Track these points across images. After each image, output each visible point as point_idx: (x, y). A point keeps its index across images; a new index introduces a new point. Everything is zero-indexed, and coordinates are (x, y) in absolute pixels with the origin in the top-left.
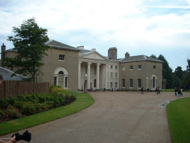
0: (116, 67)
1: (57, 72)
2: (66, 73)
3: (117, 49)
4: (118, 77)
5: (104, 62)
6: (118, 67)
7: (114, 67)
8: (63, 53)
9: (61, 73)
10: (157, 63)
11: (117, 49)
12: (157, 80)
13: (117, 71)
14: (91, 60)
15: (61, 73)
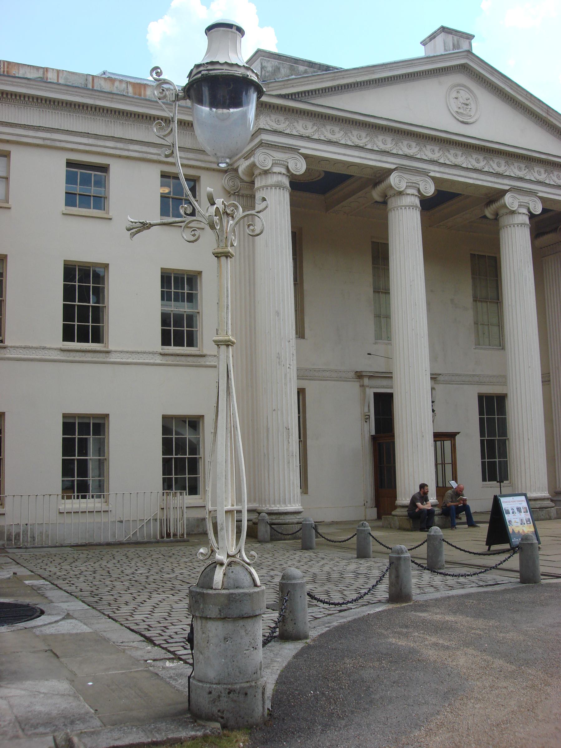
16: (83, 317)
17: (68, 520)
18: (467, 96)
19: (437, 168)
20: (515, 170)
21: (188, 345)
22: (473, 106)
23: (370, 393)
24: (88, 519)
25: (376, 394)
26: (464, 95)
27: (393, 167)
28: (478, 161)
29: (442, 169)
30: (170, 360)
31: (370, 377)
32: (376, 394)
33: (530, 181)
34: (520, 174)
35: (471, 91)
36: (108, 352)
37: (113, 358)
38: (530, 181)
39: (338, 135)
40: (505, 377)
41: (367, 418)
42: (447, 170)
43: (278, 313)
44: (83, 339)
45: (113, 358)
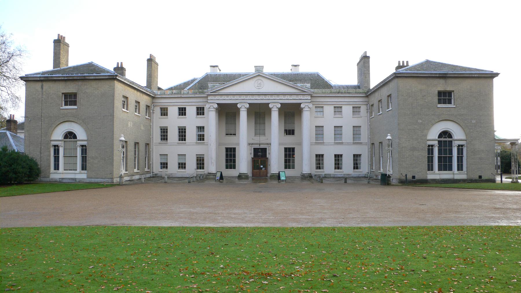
0: (356, 109)
1: (58, 134)
2: (81, 134)
3: (368, 57)
4: (365, 136)
5: (295, 97)
6: (363, 109)
7: (347, 110)
8: (70, 88)
9: (70, 135)
10: (450, 81)
11: (368, 57)
12: (461, 143)
13: (362, 120)
14: (249, 97)
15: (70, 135)
16: (182, 136)
17: (178, 173)
18: (261, 82)
19: (250, 101)
20: (273, 97)
21: (203, 141)
22: (262, 84)
23: (253, 148)
24: (182, 173)
25: (254, 148)
26: (260, 81)
27: (238, 102)
28: (262, 97)
29: (252, 101)
30: (198, 144)
31: (252, 144)
32: (254, 148)
33: (278, 100)
34: (275, 98)
35: (261, 80)
36: (186, 143)
37: (186, 144)
38: (278, 100)
39: (226, 97)
40: (279, 145)
41: (251, 154)
42: (253, 101)
43: (210, 136)
44: (182, 140)
45: (186, 144)
